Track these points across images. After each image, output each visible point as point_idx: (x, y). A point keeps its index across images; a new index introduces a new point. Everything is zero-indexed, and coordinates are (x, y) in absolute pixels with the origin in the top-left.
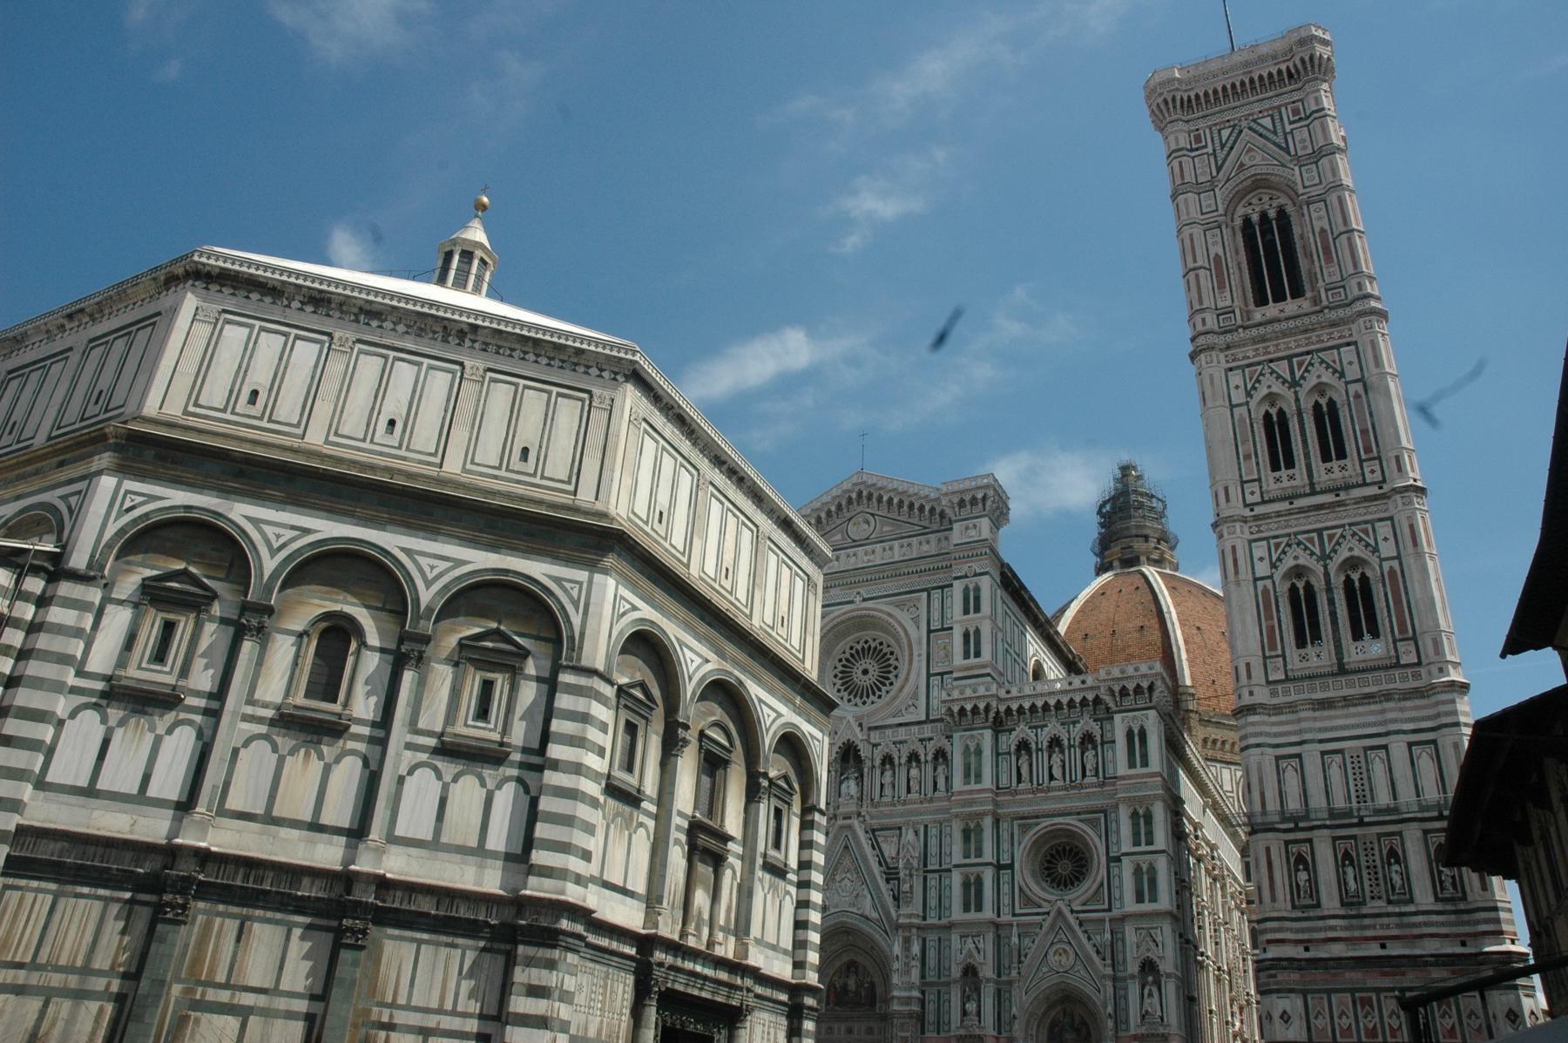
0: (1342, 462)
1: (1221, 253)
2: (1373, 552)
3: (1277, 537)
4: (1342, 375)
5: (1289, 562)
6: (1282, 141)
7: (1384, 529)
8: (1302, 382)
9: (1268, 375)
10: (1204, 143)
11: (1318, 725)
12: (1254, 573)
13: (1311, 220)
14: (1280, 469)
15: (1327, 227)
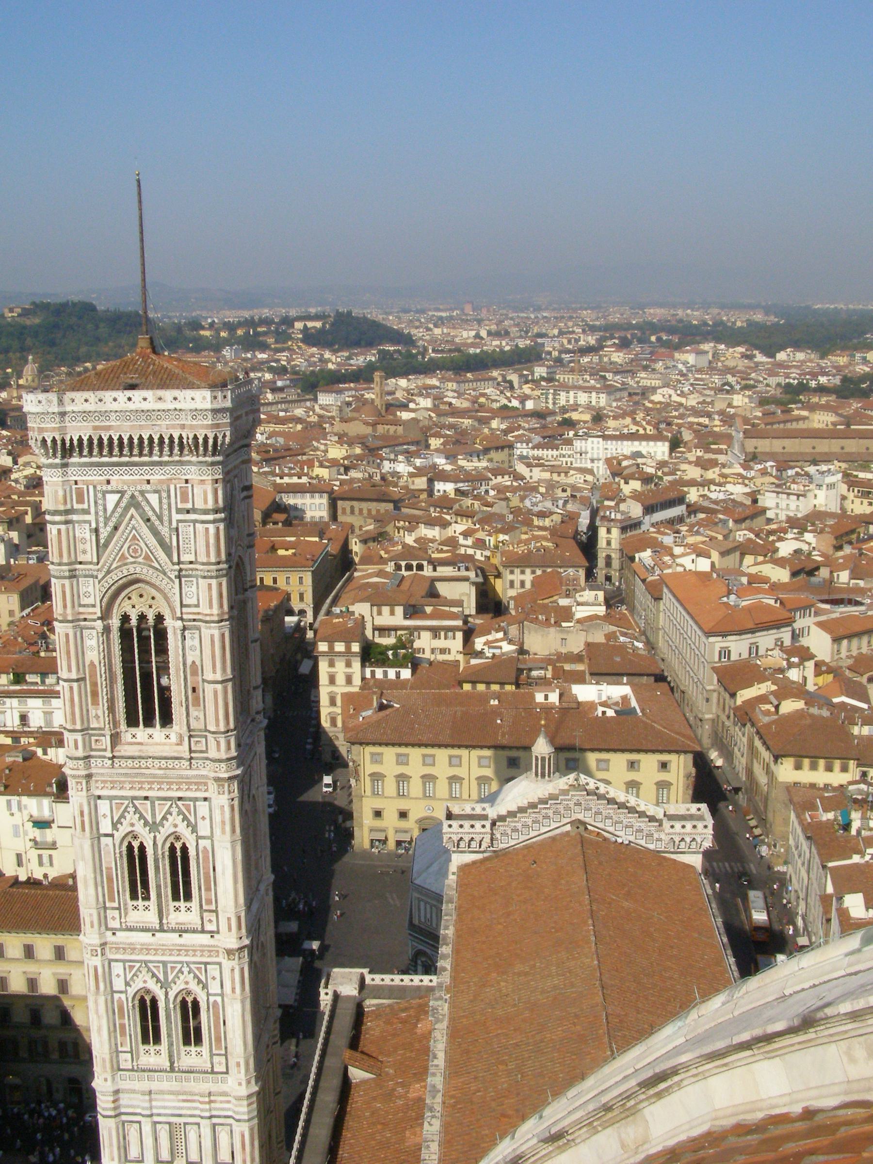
0: (188, 904)
1: (97, 664)
2: (203, 988)
3: (131, 961)
4: (194, 830)
5: (138, 985)
6: (167, 535)
7: (213, 970)
8: (160, 828)
9: (132, 813)
10: (86, 506)
11: (154, 1103)
12: (111, 987)
13: (184, 649)
14: (137, 899)
15: (198, 663)
